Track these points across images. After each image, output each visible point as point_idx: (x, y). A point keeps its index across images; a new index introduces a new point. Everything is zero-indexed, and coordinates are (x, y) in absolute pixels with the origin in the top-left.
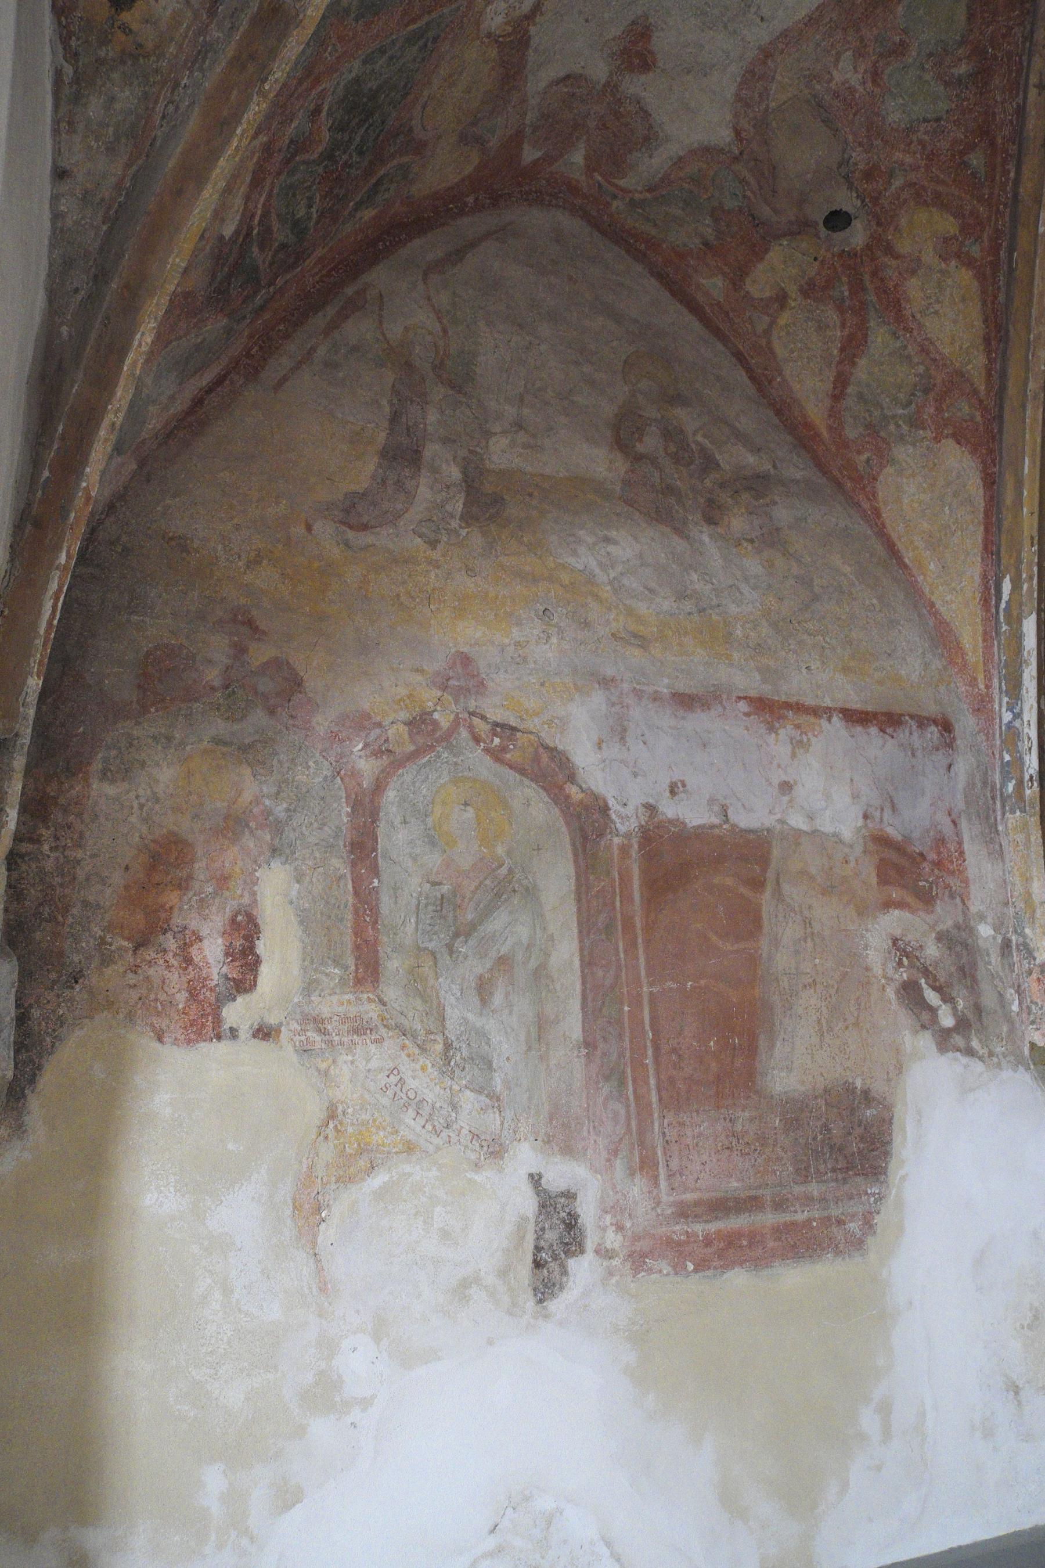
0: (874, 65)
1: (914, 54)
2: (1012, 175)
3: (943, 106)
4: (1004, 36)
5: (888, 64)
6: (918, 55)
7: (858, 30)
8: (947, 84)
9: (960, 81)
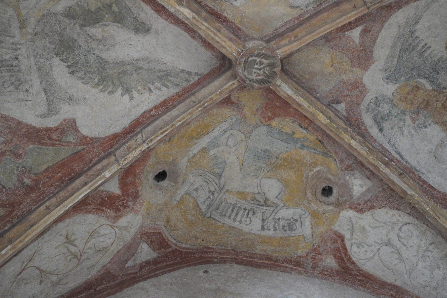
0: (6, 151)
1: (20, 161)
2: (6, 228)
3: (10, 185)
4: (48, 186)
5: (10, 155)
6: (21, 163)
7: (14, 137)
8: (19, 180)
9: (23, 183)
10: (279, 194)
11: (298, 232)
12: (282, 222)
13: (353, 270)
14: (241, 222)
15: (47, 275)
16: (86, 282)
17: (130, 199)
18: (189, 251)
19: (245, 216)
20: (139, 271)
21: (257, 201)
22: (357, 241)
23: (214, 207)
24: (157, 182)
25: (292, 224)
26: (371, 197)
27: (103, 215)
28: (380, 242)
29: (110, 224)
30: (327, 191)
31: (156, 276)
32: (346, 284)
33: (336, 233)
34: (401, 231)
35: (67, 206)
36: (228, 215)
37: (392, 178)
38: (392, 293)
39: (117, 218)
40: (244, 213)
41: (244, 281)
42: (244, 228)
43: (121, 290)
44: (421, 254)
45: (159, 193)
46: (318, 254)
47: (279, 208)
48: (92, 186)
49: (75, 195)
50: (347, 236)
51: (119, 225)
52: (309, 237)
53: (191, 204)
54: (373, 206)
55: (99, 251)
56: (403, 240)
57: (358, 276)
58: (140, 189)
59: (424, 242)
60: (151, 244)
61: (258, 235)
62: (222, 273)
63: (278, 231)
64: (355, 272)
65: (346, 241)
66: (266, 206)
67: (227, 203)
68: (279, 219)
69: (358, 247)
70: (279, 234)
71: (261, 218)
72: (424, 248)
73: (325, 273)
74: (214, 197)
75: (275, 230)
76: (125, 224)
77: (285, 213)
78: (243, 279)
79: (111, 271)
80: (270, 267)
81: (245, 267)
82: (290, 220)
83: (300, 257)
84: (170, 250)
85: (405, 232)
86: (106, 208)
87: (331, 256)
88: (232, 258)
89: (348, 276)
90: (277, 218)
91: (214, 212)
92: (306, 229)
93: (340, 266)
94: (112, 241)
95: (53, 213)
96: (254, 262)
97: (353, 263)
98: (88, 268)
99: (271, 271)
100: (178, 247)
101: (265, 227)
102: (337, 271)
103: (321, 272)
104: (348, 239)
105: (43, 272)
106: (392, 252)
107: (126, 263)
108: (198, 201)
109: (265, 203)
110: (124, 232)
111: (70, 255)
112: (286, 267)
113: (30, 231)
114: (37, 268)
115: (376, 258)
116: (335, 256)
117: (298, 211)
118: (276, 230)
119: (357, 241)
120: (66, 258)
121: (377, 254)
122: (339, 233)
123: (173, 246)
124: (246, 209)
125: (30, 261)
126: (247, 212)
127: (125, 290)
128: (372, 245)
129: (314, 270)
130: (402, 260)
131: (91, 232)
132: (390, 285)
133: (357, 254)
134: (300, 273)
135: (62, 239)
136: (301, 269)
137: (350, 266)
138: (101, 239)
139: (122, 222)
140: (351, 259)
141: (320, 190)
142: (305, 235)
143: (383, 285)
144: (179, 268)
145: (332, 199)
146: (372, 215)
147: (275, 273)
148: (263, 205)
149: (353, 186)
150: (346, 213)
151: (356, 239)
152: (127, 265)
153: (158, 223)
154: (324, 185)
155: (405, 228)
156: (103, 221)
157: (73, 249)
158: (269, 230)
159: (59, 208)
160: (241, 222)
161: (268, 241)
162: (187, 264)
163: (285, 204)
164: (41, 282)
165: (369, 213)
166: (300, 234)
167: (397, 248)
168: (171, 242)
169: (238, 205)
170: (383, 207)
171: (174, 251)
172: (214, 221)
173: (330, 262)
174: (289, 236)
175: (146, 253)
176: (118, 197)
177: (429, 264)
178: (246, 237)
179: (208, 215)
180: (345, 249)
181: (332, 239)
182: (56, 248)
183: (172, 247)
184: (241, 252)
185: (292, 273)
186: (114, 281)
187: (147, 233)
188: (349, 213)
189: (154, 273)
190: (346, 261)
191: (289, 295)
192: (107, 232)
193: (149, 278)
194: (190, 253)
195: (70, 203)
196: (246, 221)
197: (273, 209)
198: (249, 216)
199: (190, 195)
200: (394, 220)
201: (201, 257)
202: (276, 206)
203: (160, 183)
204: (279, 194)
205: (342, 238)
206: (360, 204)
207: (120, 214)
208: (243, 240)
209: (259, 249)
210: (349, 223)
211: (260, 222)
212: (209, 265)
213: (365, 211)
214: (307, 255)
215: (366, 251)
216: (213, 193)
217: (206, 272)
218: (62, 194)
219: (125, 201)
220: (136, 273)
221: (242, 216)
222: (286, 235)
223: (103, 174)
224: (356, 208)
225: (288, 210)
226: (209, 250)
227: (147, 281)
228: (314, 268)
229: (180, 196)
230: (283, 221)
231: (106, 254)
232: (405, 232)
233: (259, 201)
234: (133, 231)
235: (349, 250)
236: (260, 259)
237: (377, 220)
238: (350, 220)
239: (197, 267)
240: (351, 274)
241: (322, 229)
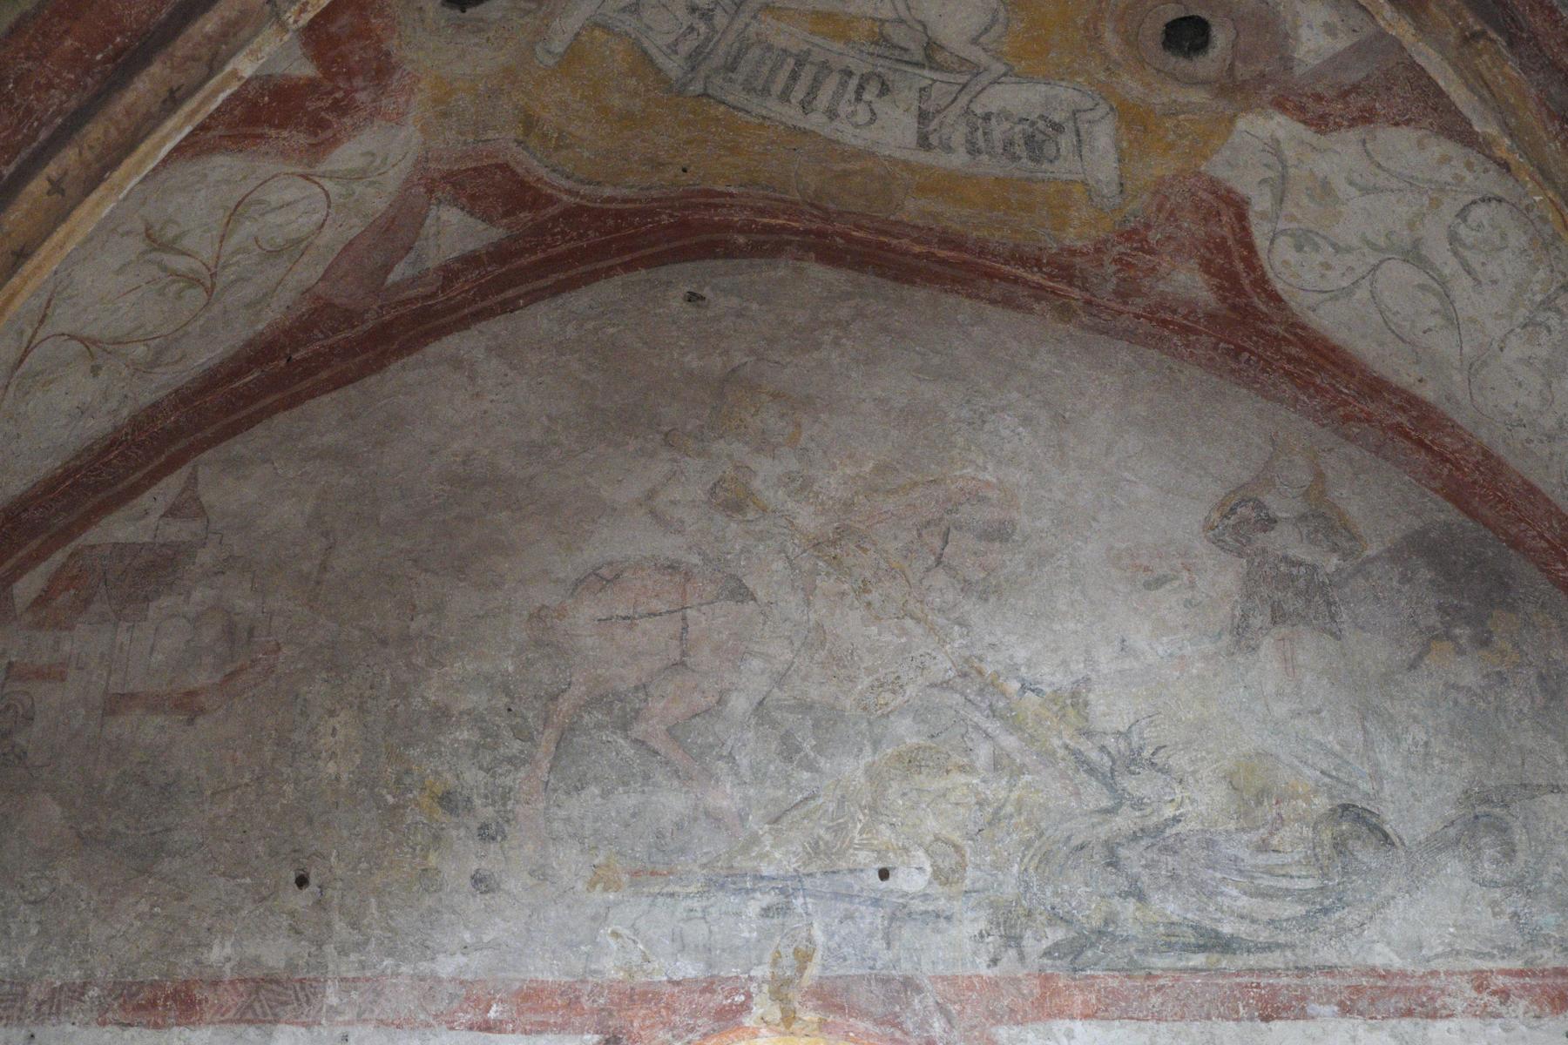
10: (986, 30)
11: (1064, 168)
12: (998, 130)
13: (1271, 322)
14: (832, 114)
15: (110, 348)
16: (249, 344)
17: (358, 82)
18: (628, 206)
19: (850, 94)
20: (443, 288)
21: (895, 47)
22: (1294, 225)
23: (717, 60)
24: (458, 13)
25: (1039, 137)
26: (1368, 76)
27: (264, 148)
28: (1382, 242)
29: (299, 170)
30: (1187, 35)
31: (508, 307)
32: (1232, 371)
33: (1214, 186)
34: (1465, 220)
35: (121, 188)
36: (777, 88)
37: (1420, 60)
38: (1401, 418)
39: (319, 150)
40: (844, 84)
41: (836, 342)
42: (851, 136)
43: (379, 365)
44: (1522, 314)
45: (476, 44)
46: (1142, 249)
47: (984, 79)
48: (194, 112)
49: (143, 148)
50: (1261, 202)
51: (330, 168)
52: (1110, 190)
53: (619, 57)
54: (1372, 110)
55: (276, 253)
56: (1467, 254)
57: (1290, 343)
58: (392, 44)
59: (1542, 274)
60: (473, 203)
61: (906, 163)
62: (755, 306)
63: (985, 157)
64: (1280, 330)
65: (1253, 218)
66: (931, 68)
67: (770, 48)
68: (987, 117)
69: (1299, 248)
70: (991, 166)
71: (914, 109)
72: (1539, 298)
73: (1168, 317)
74: (713, 29)
75: (973, 150)
76: (359, 163)
77: (1016, 99)
78: (833, 332)
79: (337, 301)
80: (954, 280)
81: (854, 274)
82: (1033, 124)
83: (1073, 252)
84: (552, 210)
85: (1480, 226)
86: (272, 125)
87: (1194, 263)
88: (807, 232)
89: (1250, 338)
90: (979, 111)
91: (718, 80)
92: (1097, 159)
93: (1224, 299)
94: (317, 218)
95: (81, 212)
96: (894, 250)
97: (1275, 297)
98: (248, 306)
99: (951, 300)
100: (583, 197)
101: (934, 140)
102: (1211, 317)
103: (1151, 315)
104: (1263, 215)
105: (95, 342)
106: (1422, 287)
107: (388, 272)
108: (646, 43)
109: (928, 57)
110: (358, 188)
111: (174, 282)
112: (1016, 280)
113: (16, 280)
114: (72, 337)
115: (1362, 294)
116: (1206, 266)
117: (1066, 95)
118: (979, 152)
119: (1294, 225)
120: (161, 292)
121: (1365, 283)
122: (1229, 191)
123: (565, 197)
124: (850, 74)
125: (41, 322)
126: (854, 83)
127: (394, 367)
128: (1349, 250)
129: (1125, 303)
130: (1452, 321)
131: (232, 205)
132: (1396, 391)
133: (1299, 273)
134: (1065, 312)
135: (136, 245)
136: (1076, 293)
137: (1263, 308)
138: (271, 218)
139: (347, 155)
140: (1267, 282)
141: (1153, 29)
142: (1091, 182)
143: (1376, 387)
144: (594, 277)
145: (1209, 63)
146: (1364, 142)
147: (965, 308)
148: (916, 64)
149: (1296, 28)
150: (1261, 121)
151: (1292, 218)
152: (393, 277)
153: (490, 135)
154: (1172, 12)
155: (1479, 213)
156: (267, 167)
157: (180, 263)
158: (949, 149)
159: (95, 196)
160: (832, 114)
161: (947, 186)
162: (627, 258)
163: (1012, 68)
164: (95, 370)
165: (1353, 135)
166: (1074, 177)
167: (1440, 275)
168: (553, 187)
169: (817, 57)
170: (1408, 123)
171: (571, 214)
172: (722, 108)
173: (1187, 282)
174: (1028, 179)
175: (454, 232)
176: (312, 85)
177: (1544, 353)
178: (856, 166)
179: (696, 87)
180: (1250, 247)
181: (1198, 208)
182: (120, 271)
183: (559, 200)
184: (840, 214)
185: (1031, 311)
186: (354, 327)
187: (449, 177)
188: (1273, 124)
189: (499, 298)
190: (1247, 288)
191: (993, 411)
192: (288, 196)
193: (479, 316)
194: (635, 213)
195: (128, 177)
196: (854, 113)
197: (963, 79)
198: (867, 96)
199: (606, 28)
200: (1446, 174)
201: (683, 226)
202: (976, 70)
203: (469, 11)
204: (986, 30)
205: (1239, 208)
206: (1319, 98)
207: (329, 133)
208: (846, 174)
209: (912, 208)
210: (1271, 160)
211: (911, 122)
212: (709, 264)
213: (1339, 126)
214: (1098, 250)
215: (1327, 266)
216: (707, 16)
217: (693, 298)
218: (95, 132)
219: (338, 95)
220: (434, 295)
221: (837, 96)
222: (1017, 174)
223: (228, 68)
224: (1302, 109)
225: (1025, 87)
226: (717, 200)
227: (474, 331)
228: (1122, 295)
229: (568, 37)
230: (1007, 125)
231: (305, 259)
232: (1480, 226)
233: (906, 50)
234: (393, 180)
235: (1263, 255)
236: (916, 241)
237: (1379, 166)
238: (1275, 148)
239: (663, 273)
240: (1261, 333)
241: (1162, 167)
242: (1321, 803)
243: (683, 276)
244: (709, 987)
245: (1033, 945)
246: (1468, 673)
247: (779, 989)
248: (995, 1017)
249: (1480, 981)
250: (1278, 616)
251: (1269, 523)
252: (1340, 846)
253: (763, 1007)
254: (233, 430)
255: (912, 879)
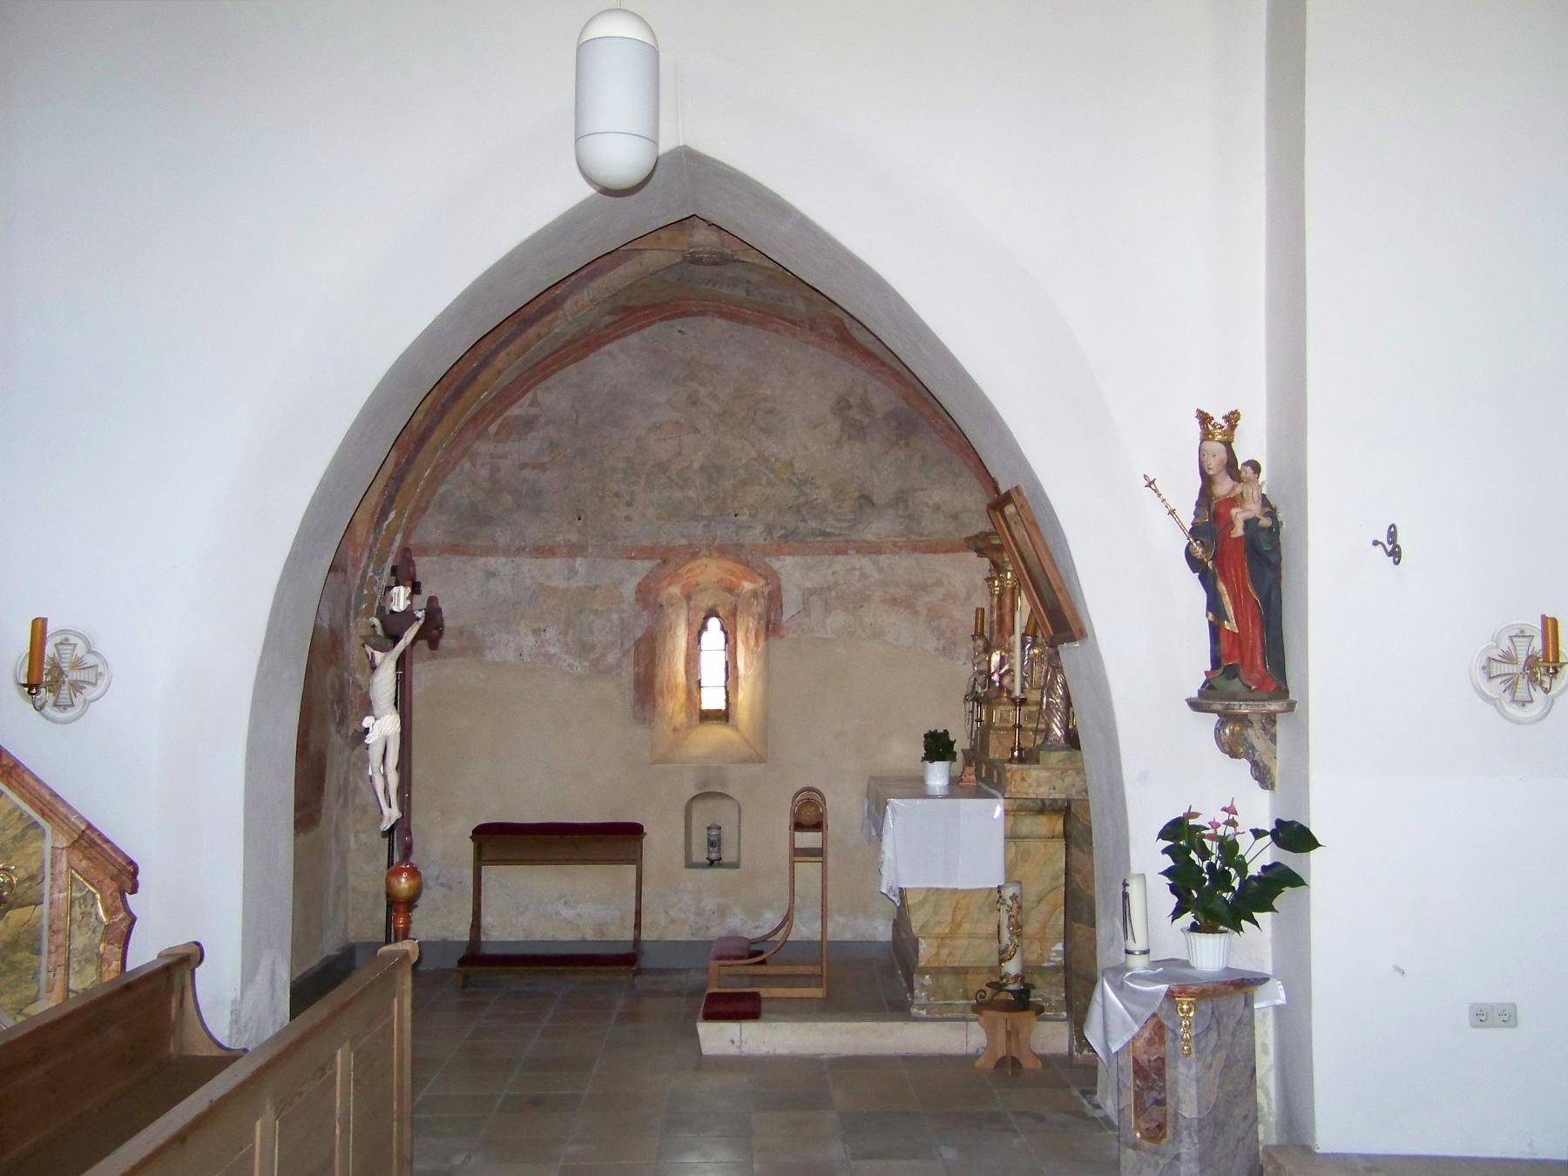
144: (650, 324)
242: (857, 494)
243: (677, 324)
244: (690, 546)
245: (776, 535)
246: (901, 455)
247: (708, 547)
248: (766, 555)
249: (894, 544)
250: (850, 437)
251: (850, 407)
252: (861, 507)
253: (704, 551)
254: (545, 377)
255: (743, 518)
